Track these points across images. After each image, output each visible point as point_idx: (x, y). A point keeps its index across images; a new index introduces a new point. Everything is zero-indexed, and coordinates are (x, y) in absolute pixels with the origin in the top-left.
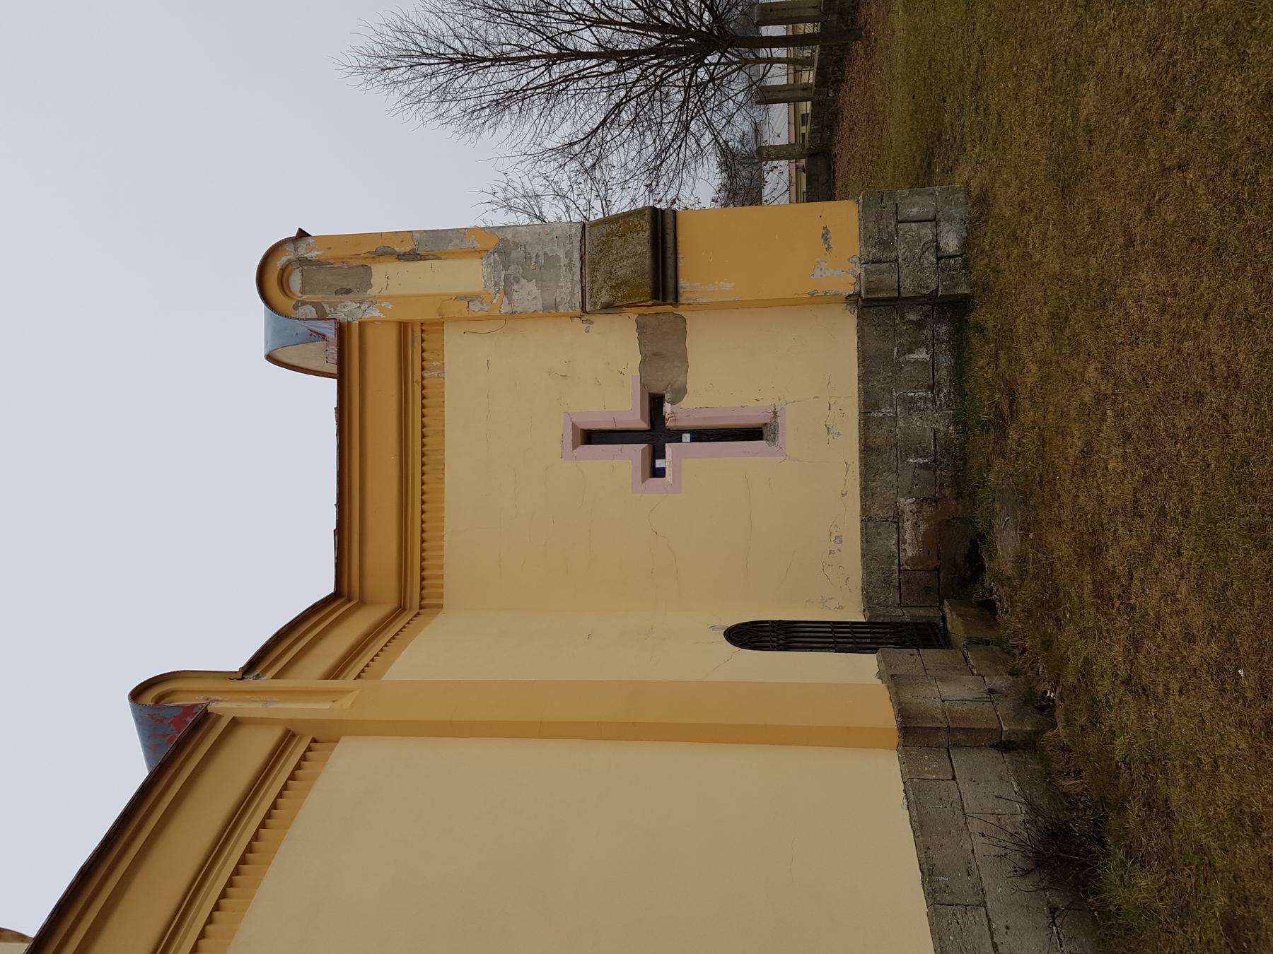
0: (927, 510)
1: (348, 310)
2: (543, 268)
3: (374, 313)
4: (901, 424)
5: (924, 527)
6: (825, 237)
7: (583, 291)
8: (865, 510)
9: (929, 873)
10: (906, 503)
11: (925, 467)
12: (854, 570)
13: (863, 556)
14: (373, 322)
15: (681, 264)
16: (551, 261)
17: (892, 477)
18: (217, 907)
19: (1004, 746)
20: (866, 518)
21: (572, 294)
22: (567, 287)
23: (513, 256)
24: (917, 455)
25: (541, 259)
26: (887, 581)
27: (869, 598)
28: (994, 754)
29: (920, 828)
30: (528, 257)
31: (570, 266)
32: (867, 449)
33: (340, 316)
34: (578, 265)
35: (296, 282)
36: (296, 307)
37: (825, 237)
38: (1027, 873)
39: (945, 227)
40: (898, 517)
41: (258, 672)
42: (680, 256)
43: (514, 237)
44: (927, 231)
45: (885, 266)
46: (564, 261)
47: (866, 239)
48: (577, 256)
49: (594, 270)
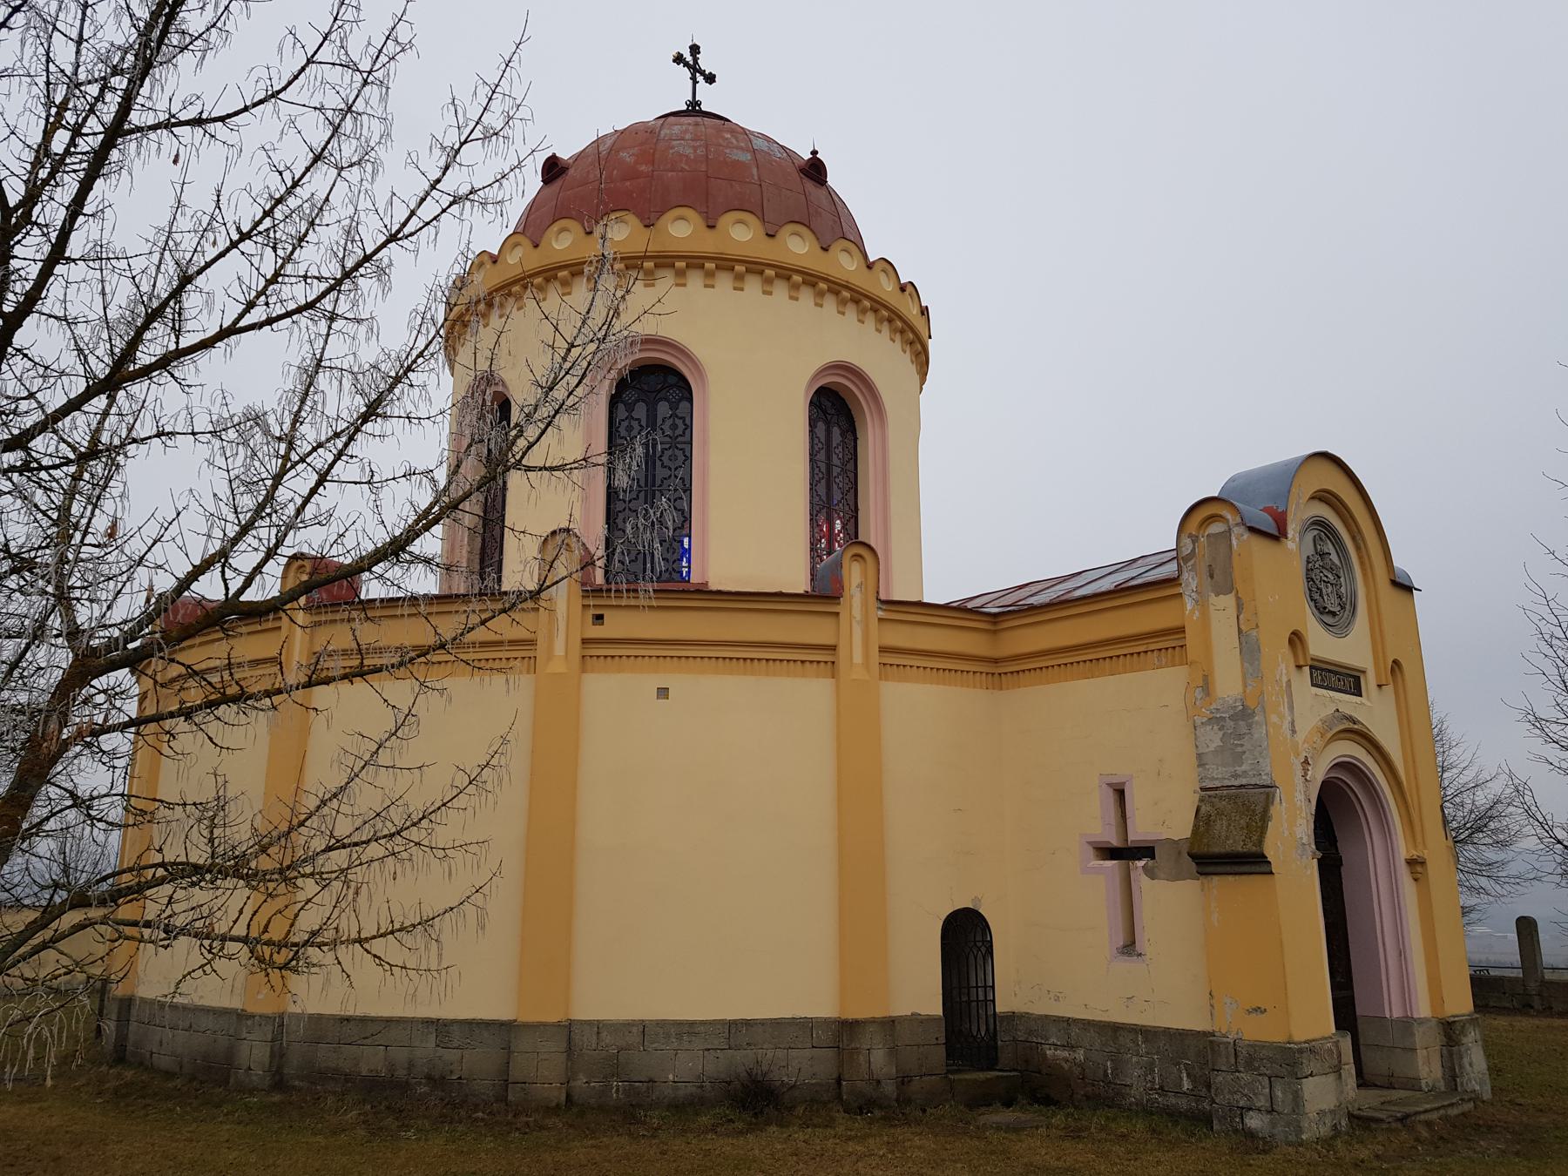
0: (1077, 1071)
1: (1190, 581)
2: (1233, 752)
3: (1189, 605)
4: (1135, 1059)
5: (1066, 1066)
6: (1258, 1010)
7: (1216, 789)
8: (1076, 1021)
9: (748, 1023)
10: (1080, 1055)
11: (1106, 1074)
12: (1039, 1009)
13: (1046, 1016)
14: (1183, 605)
15: (1230, 878)
16: (1238, 758)
17: (1097, 1046)
18: (731, 659)
19: (839, 1081)
20: (1069, 1021)
21: (1213, 779)
22: (1220, 774)
23: (1241, 723)
24: (1114, 1069)
25: (1239, 749)
26: (1030, 1032)
27: (1012, 1017)
28: (835, 1076)
29: (777, 1023)
30: (1240, 736)
31: (1236, 776)
32: (1115, 1029)
33: (1185, 575)
34: (1237, 783)
35: (1216, 528)
36: (1190, 536)
37: (1258, 1010)
38: (749, 1075)
39: (1267, 1118)
40: (1072, 1047)
42: (1237, 877)
43: (1257, 723)
44: (1262, 1102)
45: (1233, 1061)
46: (1239, 770)
47: (1256, 1046)
48: (1244, 781)
49: (1229, 797)
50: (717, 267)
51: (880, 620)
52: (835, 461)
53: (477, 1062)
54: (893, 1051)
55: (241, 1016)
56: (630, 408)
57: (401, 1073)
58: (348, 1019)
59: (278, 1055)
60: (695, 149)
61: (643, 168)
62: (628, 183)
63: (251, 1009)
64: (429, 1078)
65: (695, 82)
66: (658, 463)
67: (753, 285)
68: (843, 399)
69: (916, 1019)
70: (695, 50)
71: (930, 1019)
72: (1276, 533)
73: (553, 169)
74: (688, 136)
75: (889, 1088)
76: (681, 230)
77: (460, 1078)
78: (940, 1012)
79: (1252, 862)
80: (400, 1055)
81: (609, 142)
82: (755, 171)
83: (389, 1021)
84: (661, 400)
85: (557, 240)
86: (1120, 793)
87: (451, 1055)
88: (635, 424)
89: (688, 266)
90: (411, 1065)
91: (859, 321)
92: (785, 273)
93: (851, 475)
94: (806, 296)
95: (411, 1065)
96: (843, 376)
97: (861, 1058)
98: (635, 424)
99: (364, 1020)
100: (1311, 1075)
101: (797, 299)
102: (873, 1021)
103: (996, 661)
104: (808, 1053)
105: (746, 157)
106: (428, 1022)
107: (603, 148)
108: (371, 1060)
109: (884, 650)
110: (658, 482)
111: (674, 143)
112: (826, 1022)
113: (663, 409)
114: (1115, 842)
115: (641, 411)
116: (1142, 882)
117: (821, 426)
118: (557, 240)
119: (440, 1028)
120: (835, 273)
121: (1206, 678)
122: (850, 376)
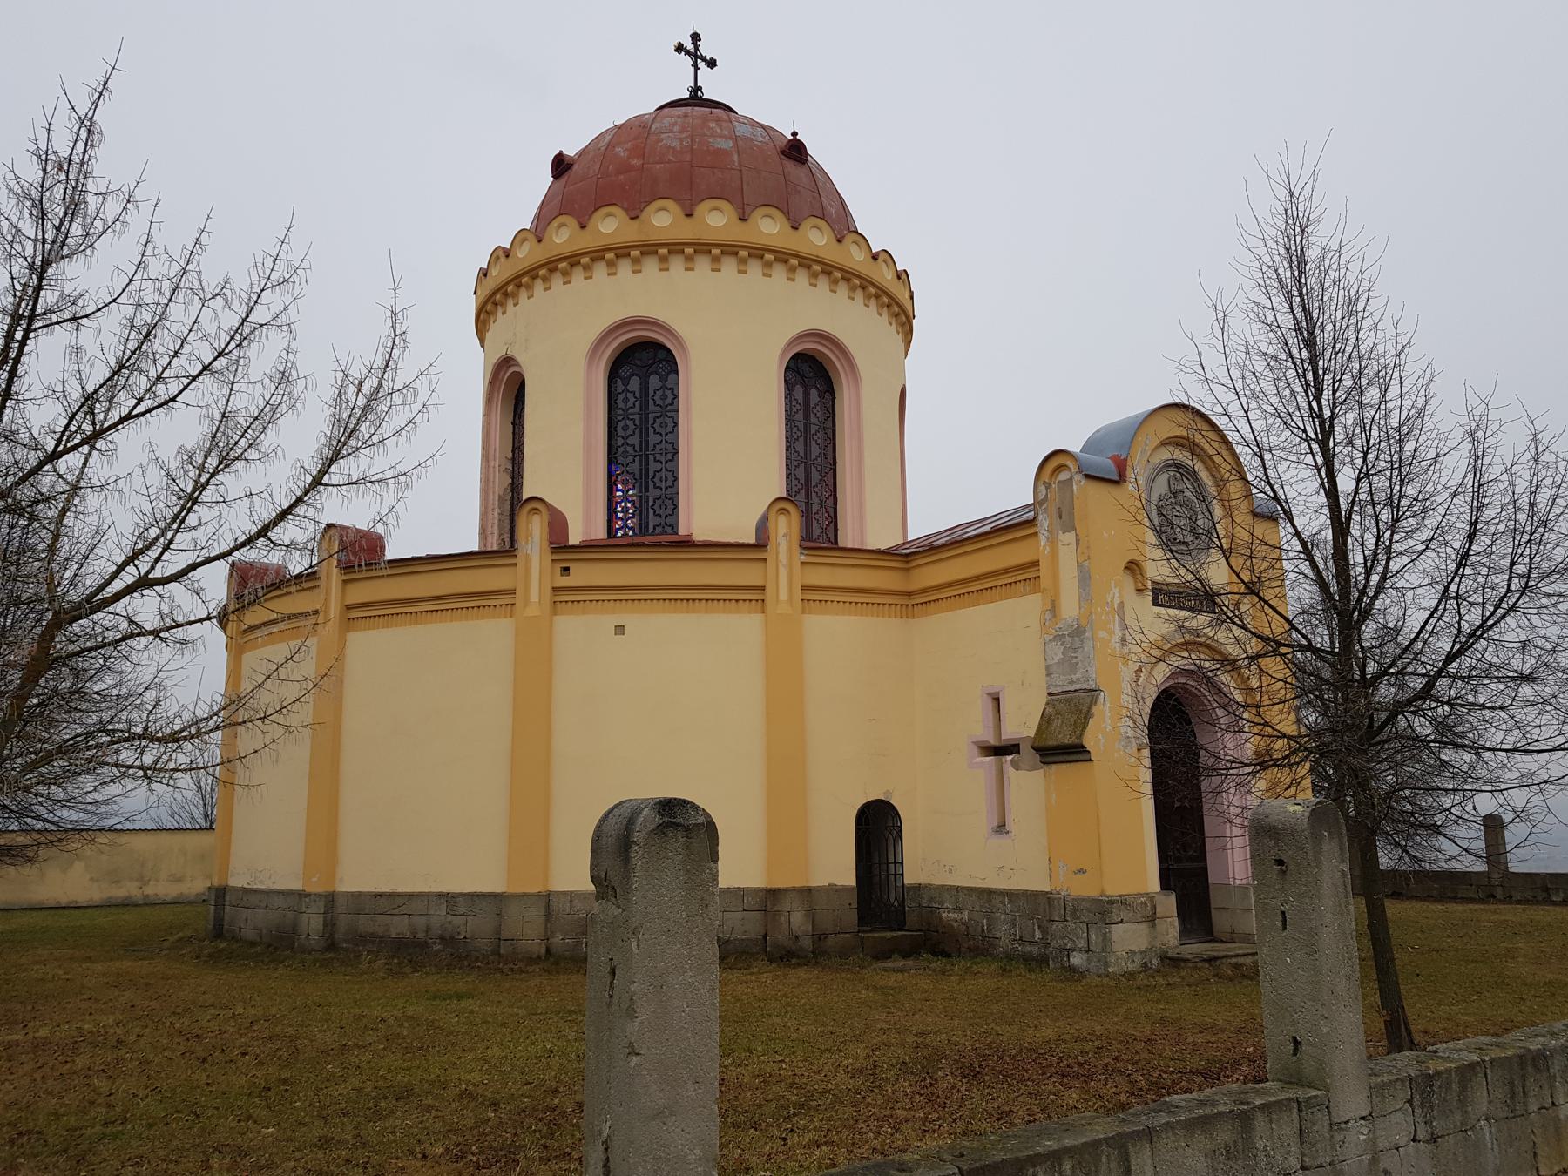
0: (963, 929)
1: (1044, 521)
2: (1069, 663)
3: (1043, 541)
4: (1003, 917)
5: (955, 925)
6: (1082, 871)
7: (1058, 694)
8: (963, 888)
10: (965, 916)
11: (983, 930)
12: (937, 882)
13: (943, 886)
14: (1039, 542)
15: (1064, 766)
16: (1073, 668)
17: (977, 908)
19: (765, 937)
20: (958, 889)
21: (1056, 686)
22: (1061, 683)
23: (1076, 639)
24: (989, 925)
25: (1075, 661)
26: (931, 899)
27: (918, 888)
28: (763, 933)
30: (1075, 650)
31: (1072, 682)
32: (990, 893)
33: (1040, 517)
34: (1073, 689)
35: (1063, 476)
36: (1044, 483)
37: (1082, 871)
39: (1085, 956)
40: (960, 910)
41: (806, 552)
42: (1068, 765)
43: (1088, 638)
44: (1082, 944)
45: (1063, 912)
46: (1074, 677)
47: (1079, 900)
48: (1077, 687)
49: (1066, 700)
50: (695, 252)
51: (802, 563)
52: (813, 419)
53: (476, 926)
54: (811, 914)
55: (301, 895)
56: (626, 382)
57: (421, 935)
58: (380, 895)
59: (330, 925)
60: (681, 140)
61: (635, 162)
62: (621, 177)
63: (308, 890)
64: (442, 938)
65: (696, 68)
66: (651, 430)
67: (729, 266)
68: (821, 363)
69: (833, 890)
70: (696, 37)
71: (845, 889)
72: (1117, 478)
73: (561, 165)
74: (676, 128)
75: (806, 943)
76: (663, 220)
77: (465, 938)
78: (854, 884)
79: (1074, 752)
80: (420, 921)
81: (608, 138)
82: (736, 157)
83: (411, 895)
84: (651, 374)
85: (557, 235)
86: (997, 700)
87: (458, 920)
88: (630, 396)
89: (669, 252)
90: (428, 929)
91: (832, 291)
92: (757, 252)
93: (830, 432)
94: (779, 272)
95: (428, 929)
96: (819, 343)
97: (783, 918)
98: (630, 396)
99: (392, 895)
100: (1122, 922)
101: (770, 276)
102: (793, 889)
103: (909, 594)
104: (739, 915)
105: (727, 145)
106: (440, 895)
107: (603, 144)
108: (398, 926)
109: (805, 588)
110: (651, 448)
111: (663, 136)
112: (756, 891)
113: (654, 381)
114: (993, 742)
115: (635, 384)
116: (1010, 771)
117: (799, 390)
118: (557, 235)
119: (449, 898)
120: (804, 249)
121: (1053, 602)
122: (828, 344)
